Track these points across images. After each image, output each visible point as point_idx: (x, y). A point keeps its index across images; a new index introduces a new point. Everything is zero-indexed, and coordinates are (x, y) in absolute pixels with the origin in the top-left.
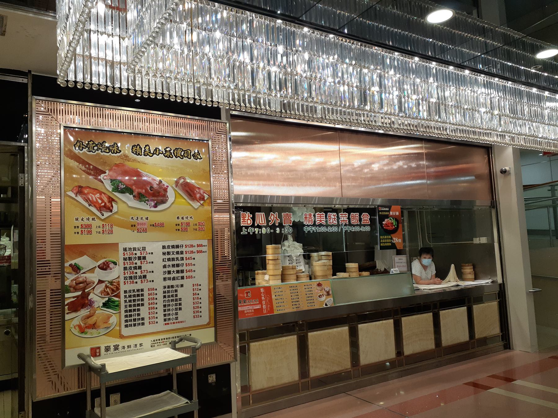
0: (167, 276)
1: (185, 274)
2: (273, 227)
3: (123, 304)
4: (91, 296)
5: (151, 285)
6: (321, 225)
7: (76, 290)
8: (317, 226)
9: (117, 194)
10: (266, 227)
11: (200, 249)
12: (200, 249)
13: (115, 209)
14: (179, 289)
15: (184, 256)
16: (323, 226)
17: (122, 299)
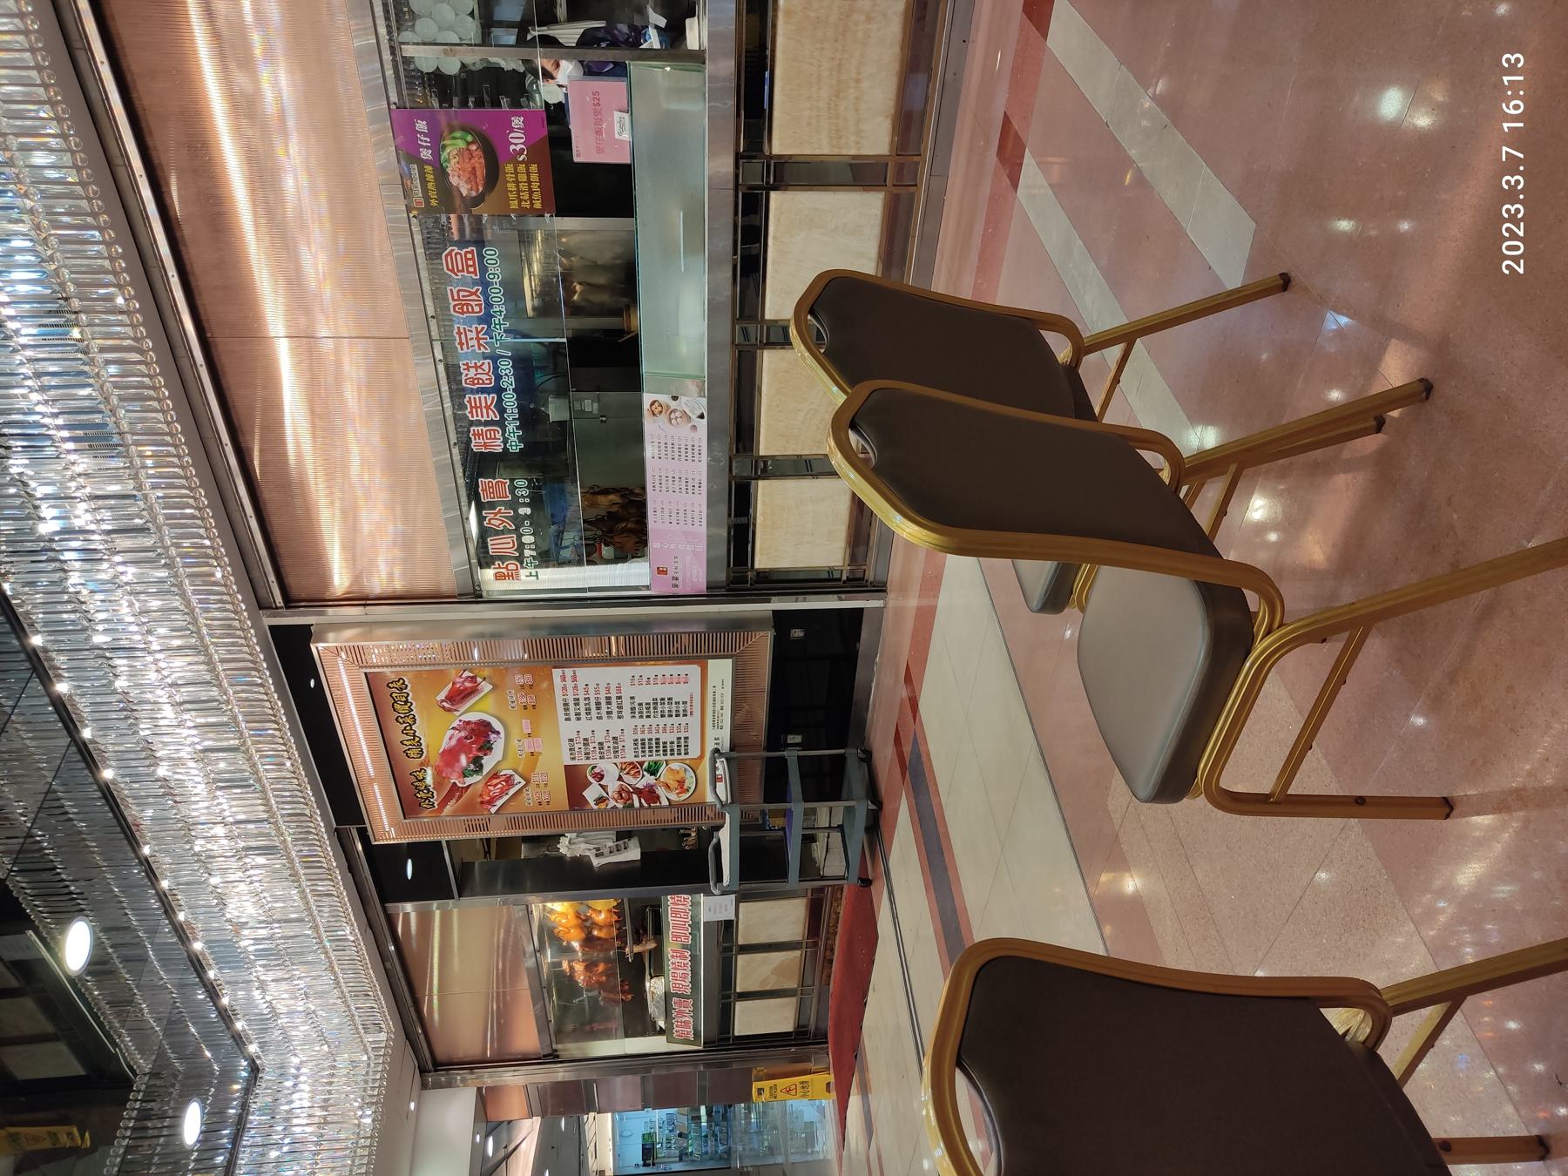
0: (615, 715)
2: (518, 520)
3: (655, 758)
4: (640, 786)
7: (630, 798)
8: (503, 419)
10: (520, 536)
14: (637, 701)
16: (500, 400)
17: (647, 759)
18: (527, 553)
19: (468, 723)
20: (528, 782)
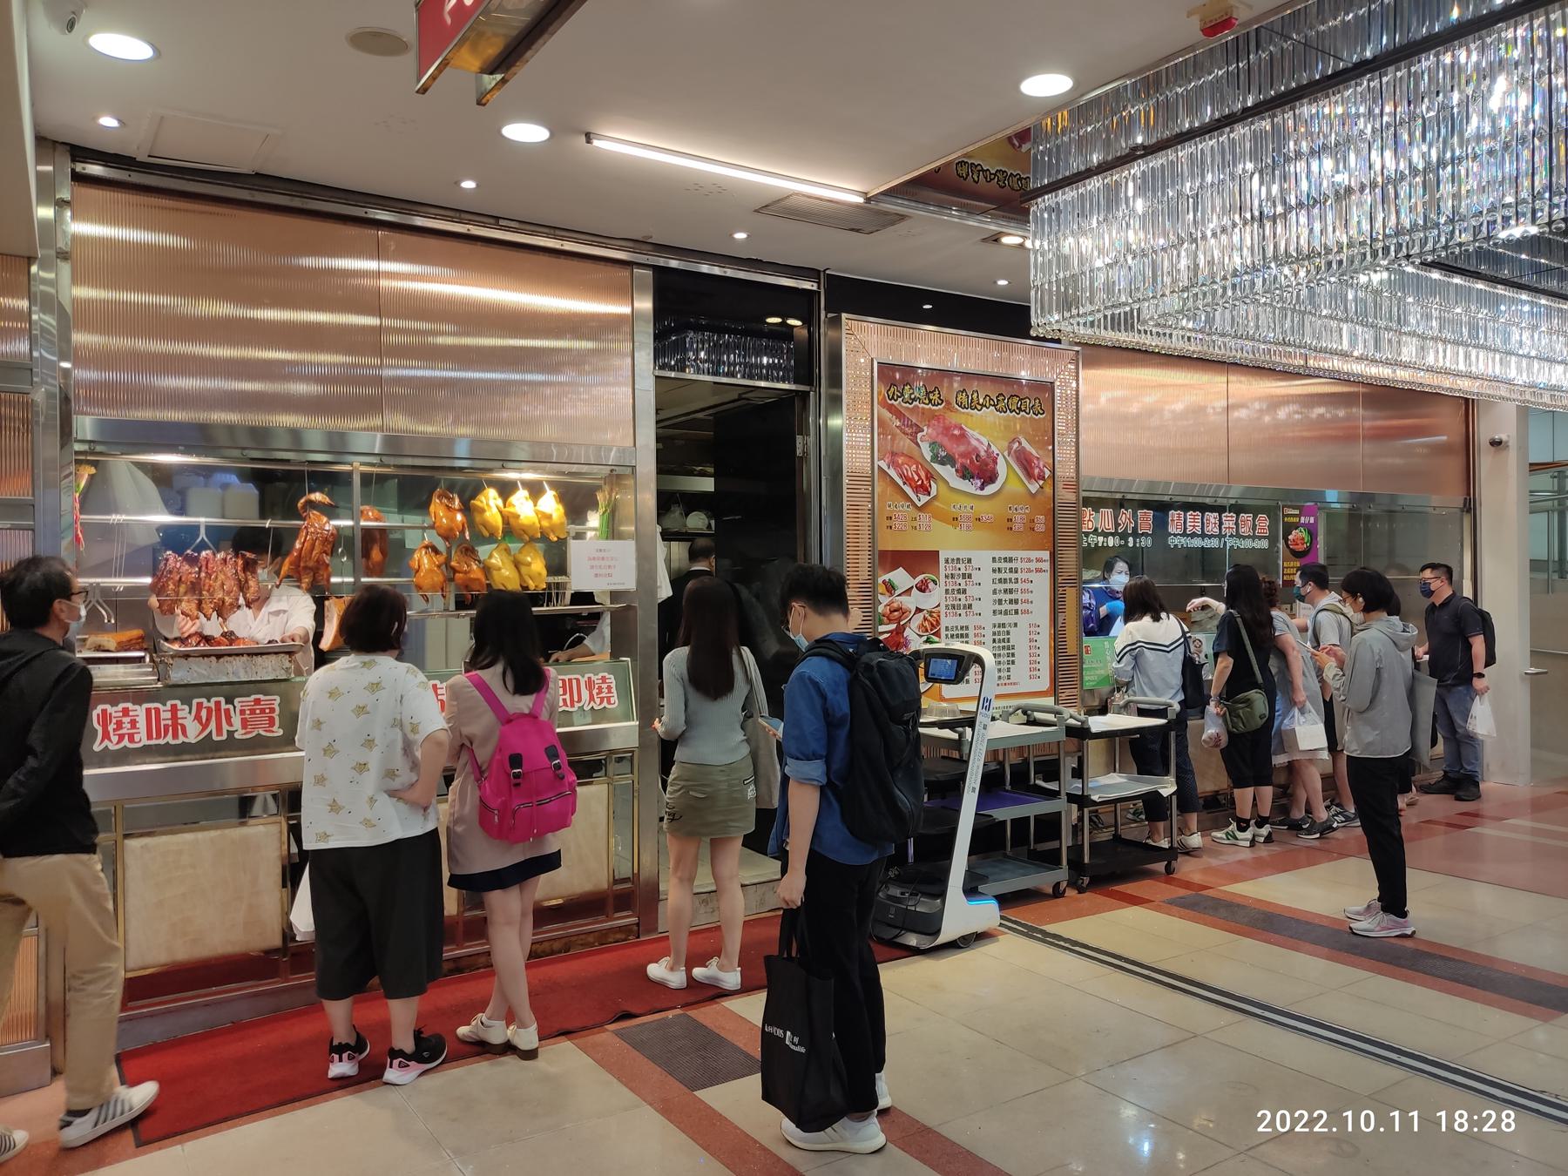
0: (997, 607)
1: (1019, 607)
2: (1124, 536)
4: (907, 632)
5: (977, 621)
6: (1193, 535)
7: (890, 621)
9: (936, 466)
10: (1112, 534)
11: (1039, 565)
12: (1039, 565)
13: (934, 492)
14: (1012, 630)
15: (1019, 575)
18: (1101, 539)
19: (995, 462)
20: (920, 509)
